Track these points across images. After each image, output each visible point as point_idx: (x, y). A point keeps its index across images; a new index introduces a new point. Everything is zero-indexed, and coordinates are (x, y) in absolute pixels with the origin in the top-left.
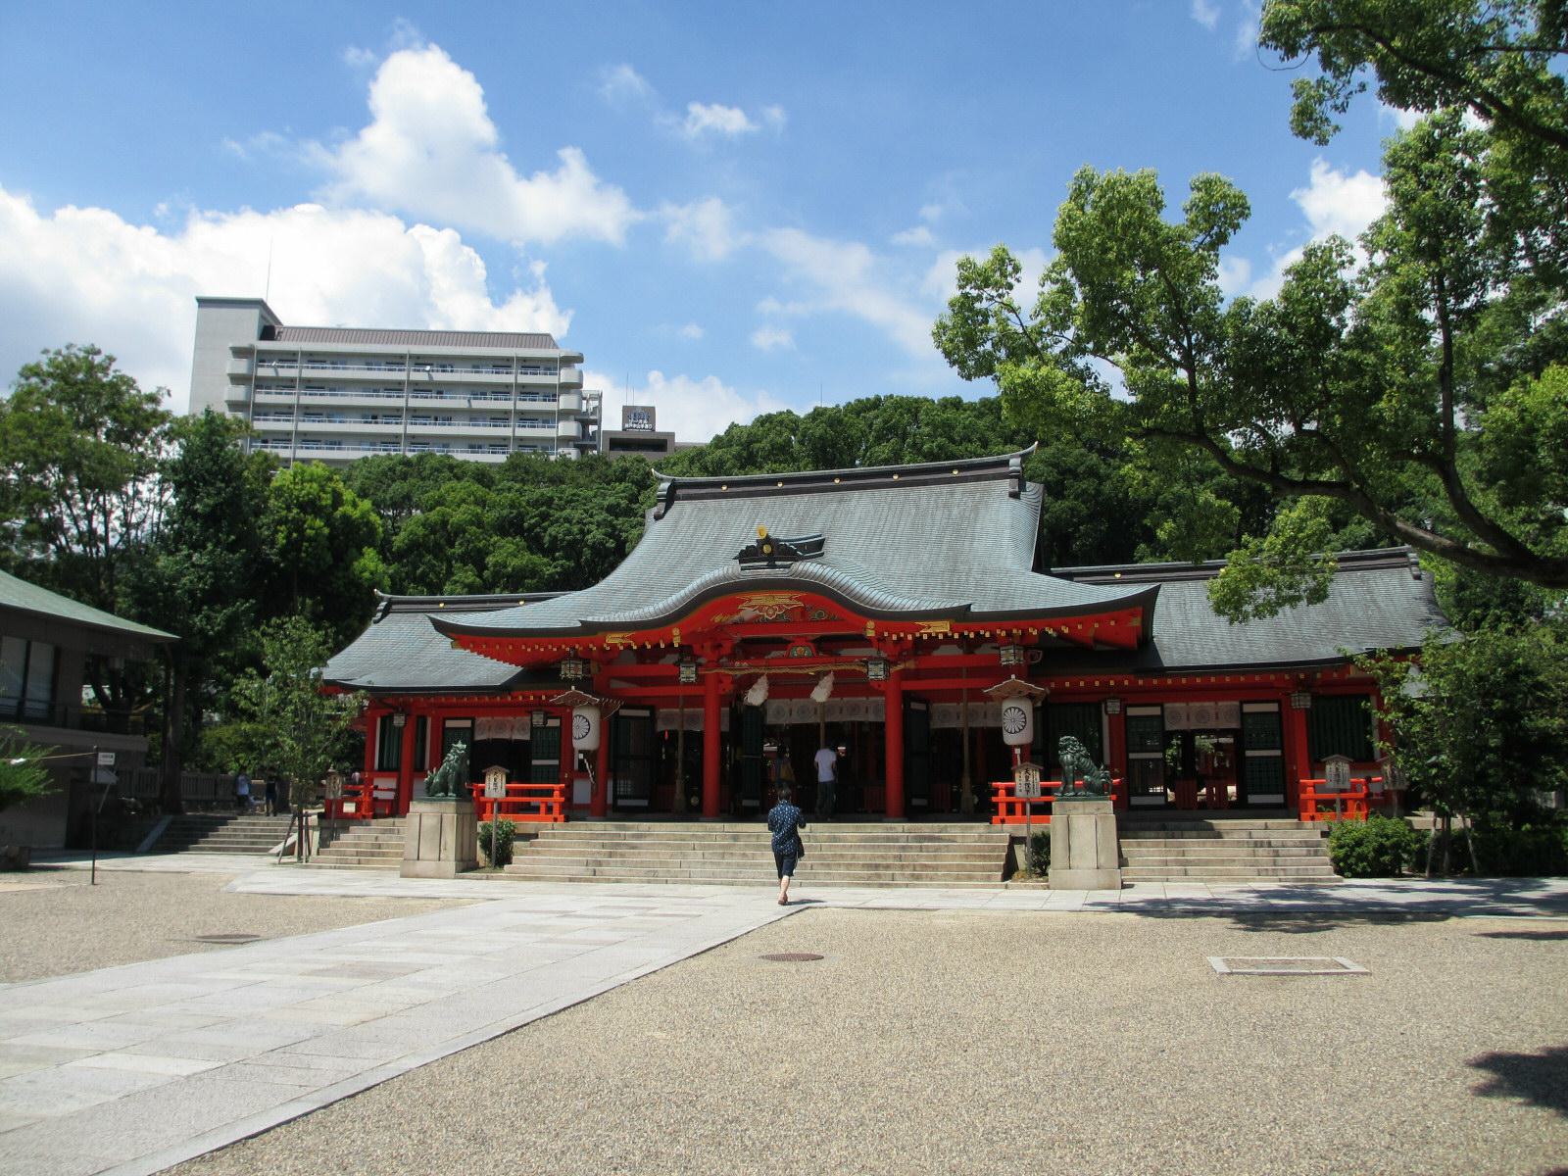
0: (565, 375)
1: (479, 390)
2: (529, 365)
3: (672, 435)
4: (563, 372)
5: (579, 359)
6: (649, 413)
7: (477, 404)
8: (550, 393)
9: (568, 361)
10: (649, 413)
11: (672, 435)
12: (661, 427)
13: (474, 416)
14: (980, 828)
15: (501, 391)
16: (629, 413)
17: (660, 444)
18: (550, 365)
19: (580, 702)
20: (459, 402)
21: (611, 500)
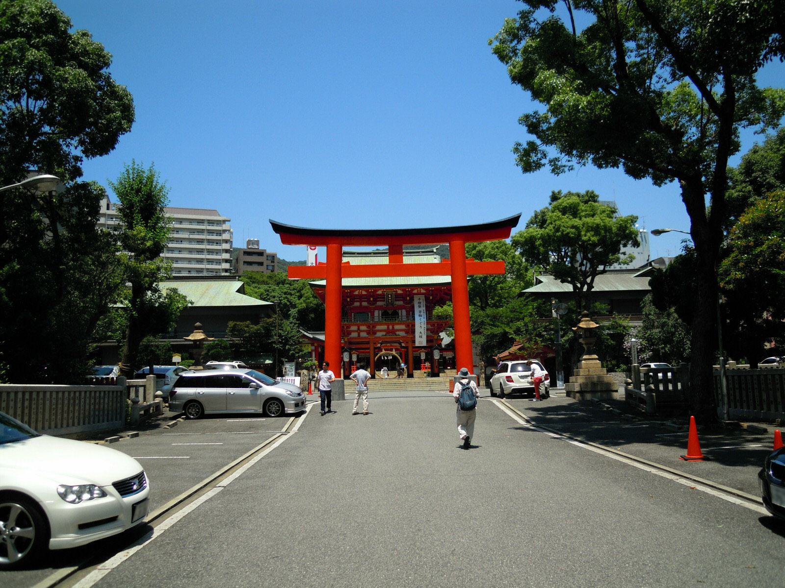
0: (225, 227)
1: (192, 231)
2: (211, 222)
3: (266, 250)
4: (224, 226)
5: (229, 221)
6: (257, 243)
7: (192, 236)
8: (219, 233)
9: (224, 221)
10: (257, 243)
11: (266, 250)
12: (262, 247)
13: (190, 240)
14: (419, 371)
15: (201, 231)
16: (249, 242)
17: (261, 254)
18: (219, 222)
19: (354, 353)
20: (185, 235)
21: (285, 290)
